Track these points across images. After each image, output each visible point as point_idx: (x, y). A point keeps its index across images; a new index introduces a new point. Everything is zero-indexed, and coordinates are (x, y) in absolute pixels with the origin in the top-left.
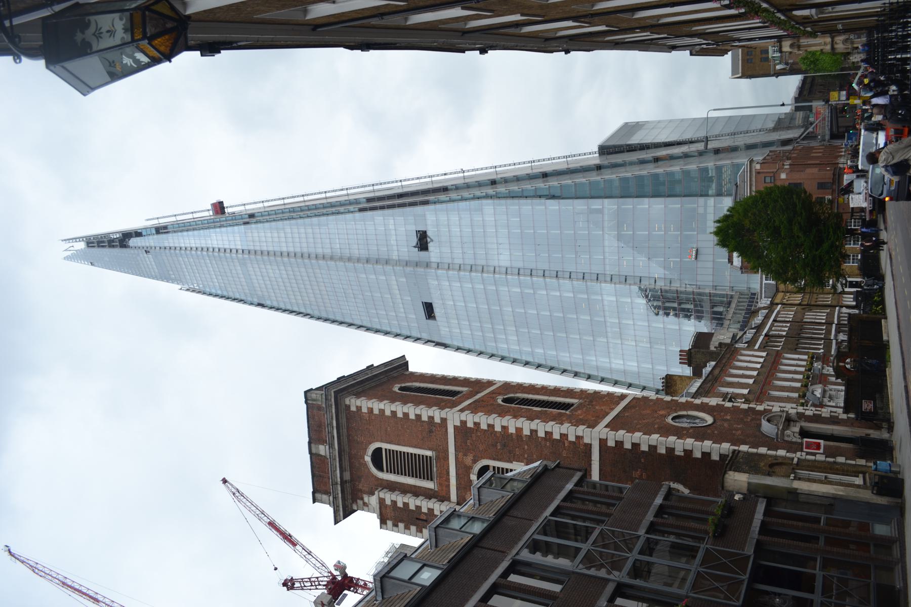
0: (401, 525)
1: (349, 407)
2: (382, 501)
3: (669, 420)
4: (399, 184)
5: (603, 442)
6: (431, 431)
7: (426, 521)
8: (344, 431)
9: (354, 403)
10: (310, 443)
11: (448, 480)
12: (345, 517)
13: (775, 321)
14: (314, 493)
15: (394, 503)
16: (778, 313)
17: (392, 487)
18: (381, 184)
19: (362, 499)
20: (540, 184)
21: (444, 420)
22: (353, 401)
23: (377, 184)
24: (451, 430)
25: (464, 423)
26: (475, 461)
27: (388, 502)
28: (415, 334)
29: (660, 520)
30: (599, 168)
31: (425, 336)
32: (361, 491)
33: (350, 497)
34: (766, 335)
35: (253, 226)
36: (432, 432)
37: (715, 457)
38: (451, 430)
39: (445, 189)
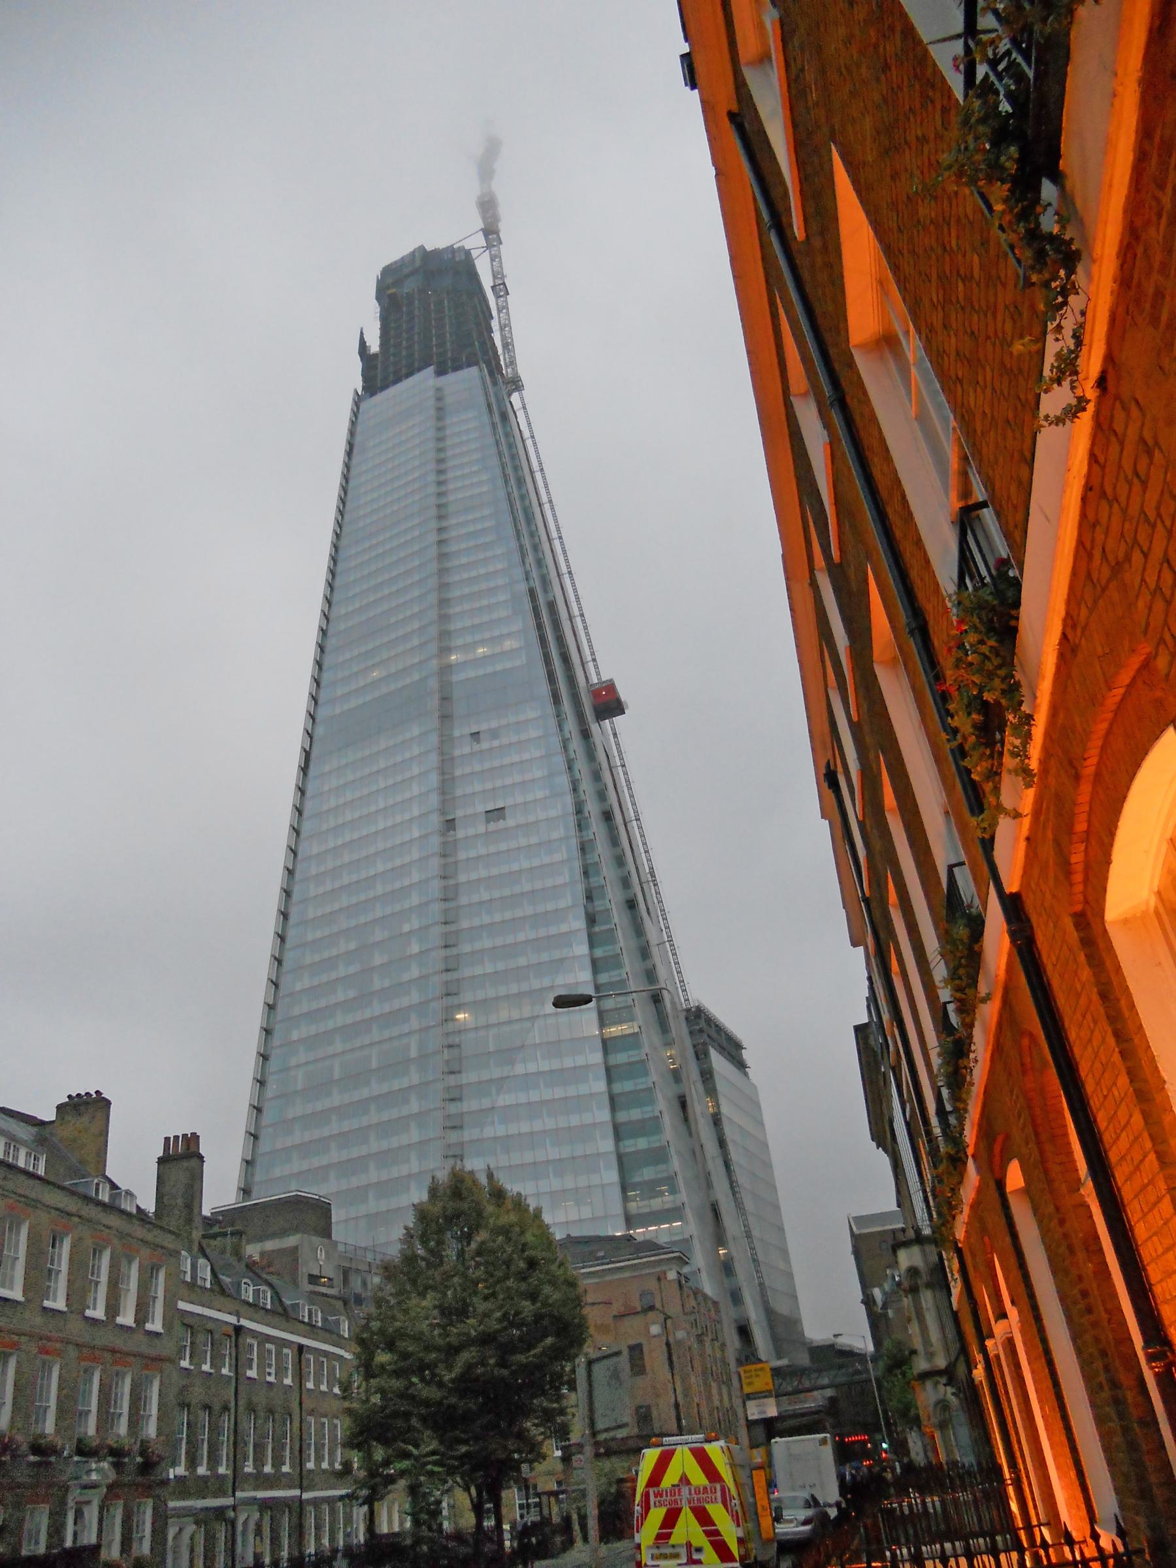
4: (589, 658)
13: (301, 1348)
16: (340, 1358)
18: (586, 628)
20: (613, 898)
23: (584, 621)
28: (321, 714)
31: (320, 731)
34: (238, 1329)
35: (486, 419)
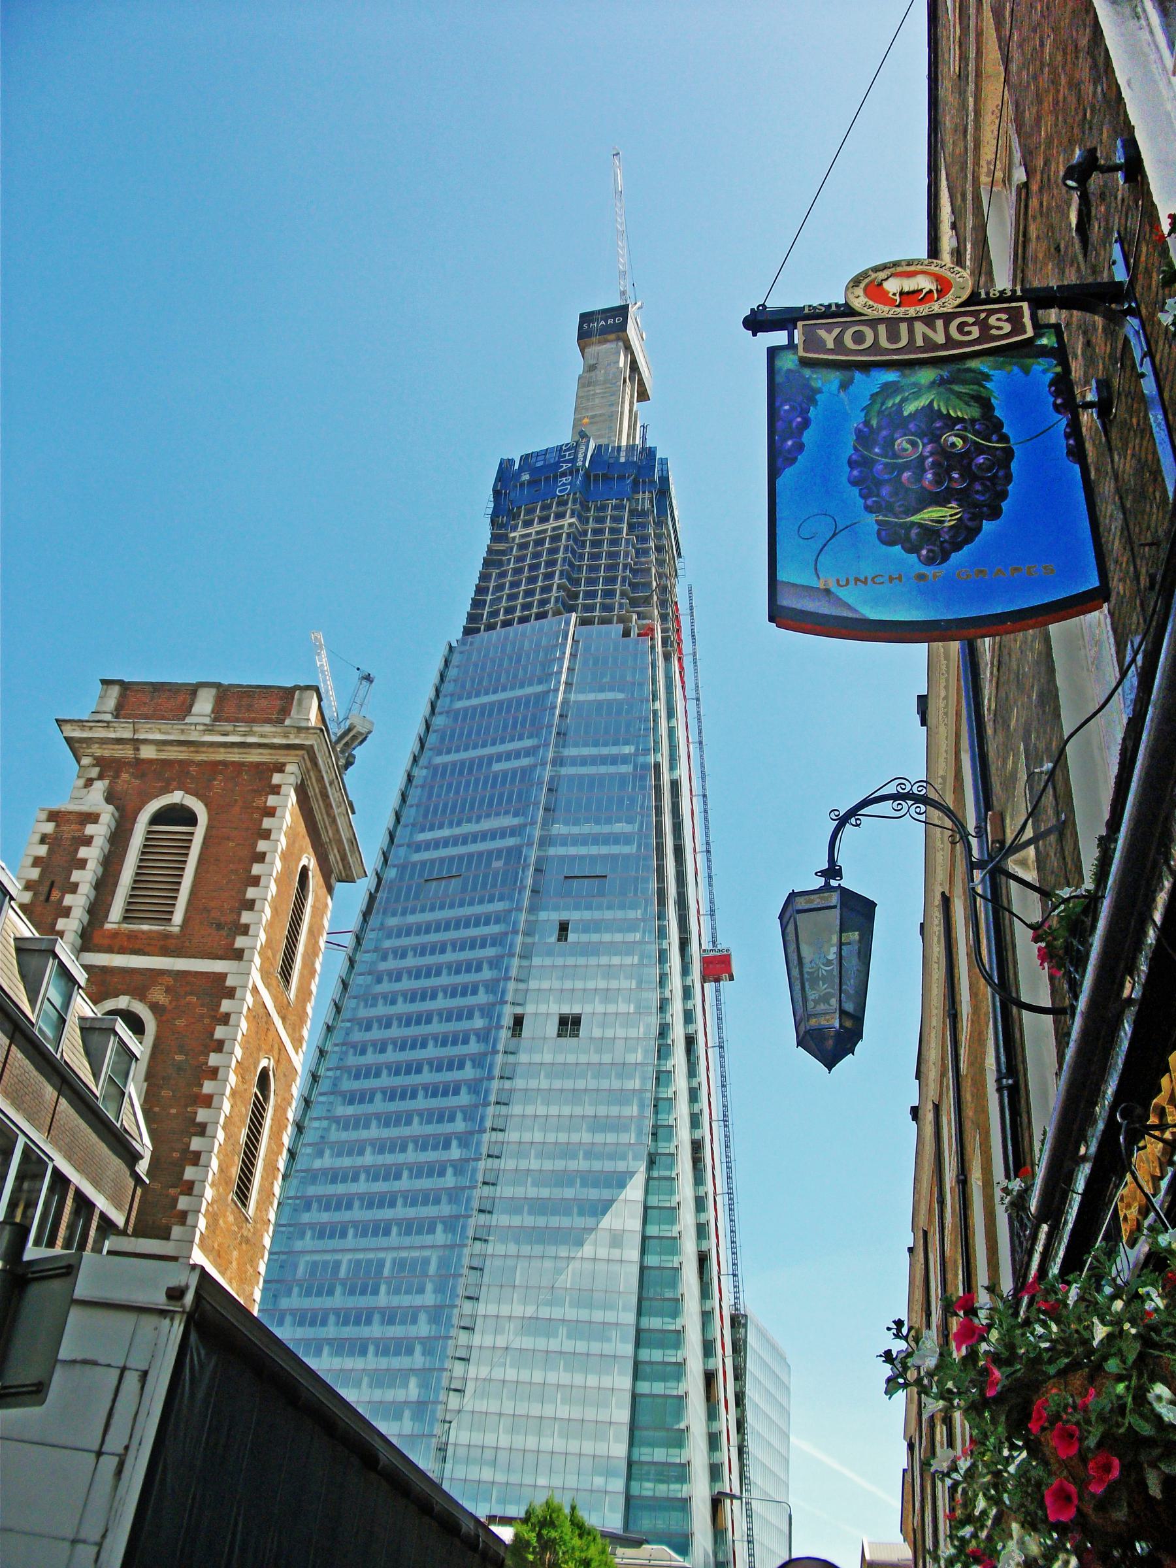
1: (280, 768)
2: (93, 818)
6: (219, 927)
7: (47, 899)
8: (235, 756)
9: (287, 780)
10: (218, 686)
11: (122, 951)
14: (120, 683)
15: (88, 841)
17: (119, 838)
19: (101, 777)
21: (238, 955)
22: (292, 780)
25: (230, 993)
26: (155, 1008)
27: (90, 829)
32: (117, 776)
33: (107, 753)
36: (221, 928)
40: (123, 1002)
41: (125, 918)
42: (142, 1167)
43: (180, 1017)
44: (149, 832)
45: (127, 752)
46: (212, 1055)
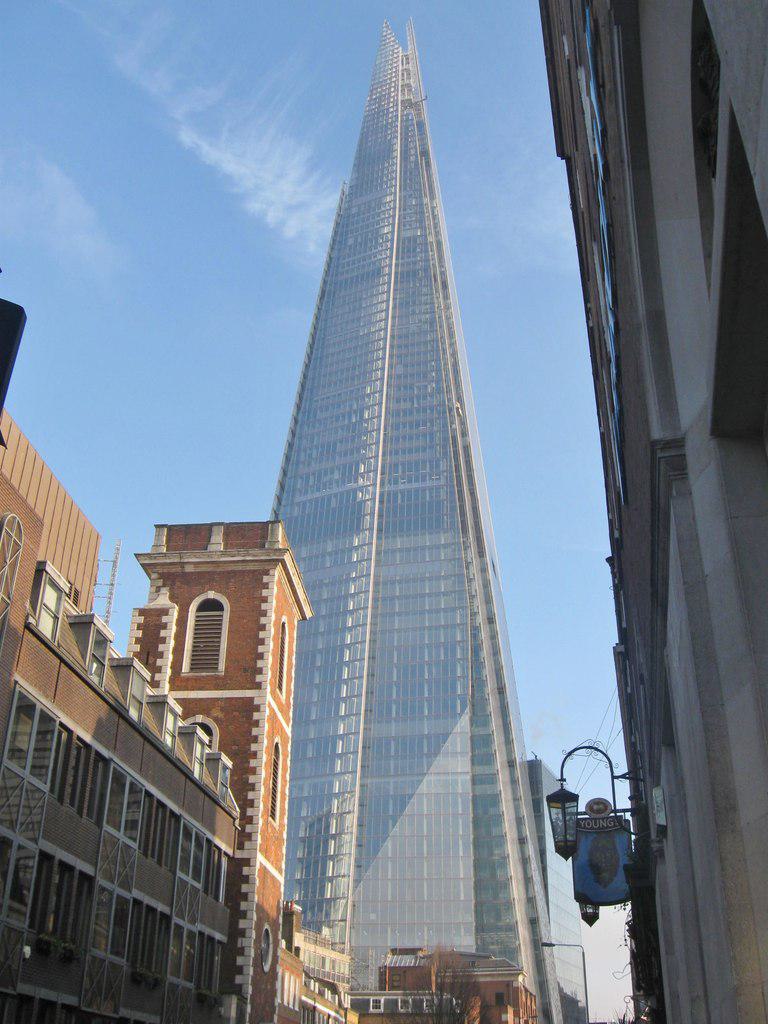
0: (140, 634)
1: (267, 573)
2: (165, 612)
3: (267, 926)
5: (247, 862)
6: (245, 670)
8: (240, 567)
12: (144, 566)
19: (164, 585)
20: (490, 686)
21: (258, 686)
24: (248, 693)
25: (257, 708)
26: (216, 720)
27: (164, 619)
29: (158, 917)
30: (511, 764)
33: (165, 571)
36: (247, 671)
37: (238, 979)
38: (248, 693)
39: (481, 553)
40: (200, 718)
41: (191, 669)
42: (237, 822)
43: (231, 724)
44: (197, 617)
45: (179, 569)
46: (252, 745)
